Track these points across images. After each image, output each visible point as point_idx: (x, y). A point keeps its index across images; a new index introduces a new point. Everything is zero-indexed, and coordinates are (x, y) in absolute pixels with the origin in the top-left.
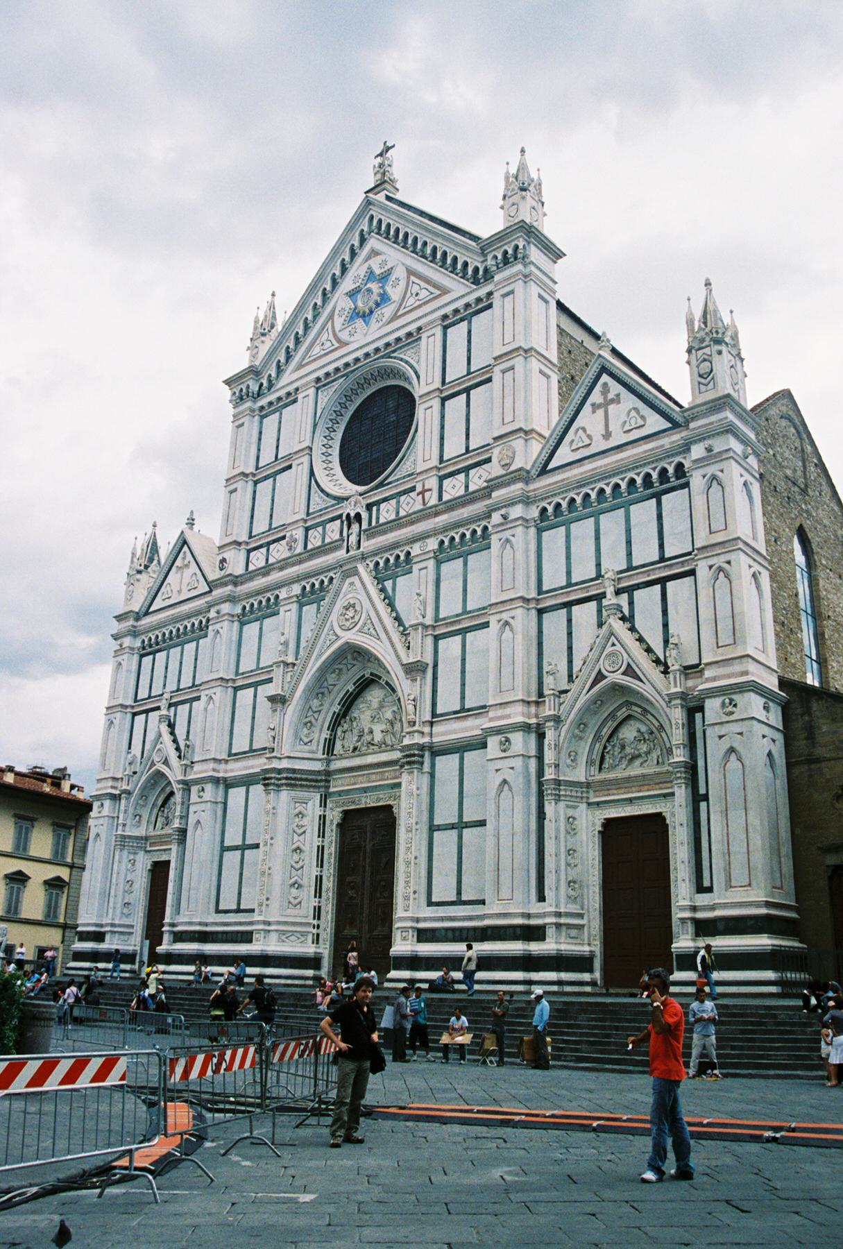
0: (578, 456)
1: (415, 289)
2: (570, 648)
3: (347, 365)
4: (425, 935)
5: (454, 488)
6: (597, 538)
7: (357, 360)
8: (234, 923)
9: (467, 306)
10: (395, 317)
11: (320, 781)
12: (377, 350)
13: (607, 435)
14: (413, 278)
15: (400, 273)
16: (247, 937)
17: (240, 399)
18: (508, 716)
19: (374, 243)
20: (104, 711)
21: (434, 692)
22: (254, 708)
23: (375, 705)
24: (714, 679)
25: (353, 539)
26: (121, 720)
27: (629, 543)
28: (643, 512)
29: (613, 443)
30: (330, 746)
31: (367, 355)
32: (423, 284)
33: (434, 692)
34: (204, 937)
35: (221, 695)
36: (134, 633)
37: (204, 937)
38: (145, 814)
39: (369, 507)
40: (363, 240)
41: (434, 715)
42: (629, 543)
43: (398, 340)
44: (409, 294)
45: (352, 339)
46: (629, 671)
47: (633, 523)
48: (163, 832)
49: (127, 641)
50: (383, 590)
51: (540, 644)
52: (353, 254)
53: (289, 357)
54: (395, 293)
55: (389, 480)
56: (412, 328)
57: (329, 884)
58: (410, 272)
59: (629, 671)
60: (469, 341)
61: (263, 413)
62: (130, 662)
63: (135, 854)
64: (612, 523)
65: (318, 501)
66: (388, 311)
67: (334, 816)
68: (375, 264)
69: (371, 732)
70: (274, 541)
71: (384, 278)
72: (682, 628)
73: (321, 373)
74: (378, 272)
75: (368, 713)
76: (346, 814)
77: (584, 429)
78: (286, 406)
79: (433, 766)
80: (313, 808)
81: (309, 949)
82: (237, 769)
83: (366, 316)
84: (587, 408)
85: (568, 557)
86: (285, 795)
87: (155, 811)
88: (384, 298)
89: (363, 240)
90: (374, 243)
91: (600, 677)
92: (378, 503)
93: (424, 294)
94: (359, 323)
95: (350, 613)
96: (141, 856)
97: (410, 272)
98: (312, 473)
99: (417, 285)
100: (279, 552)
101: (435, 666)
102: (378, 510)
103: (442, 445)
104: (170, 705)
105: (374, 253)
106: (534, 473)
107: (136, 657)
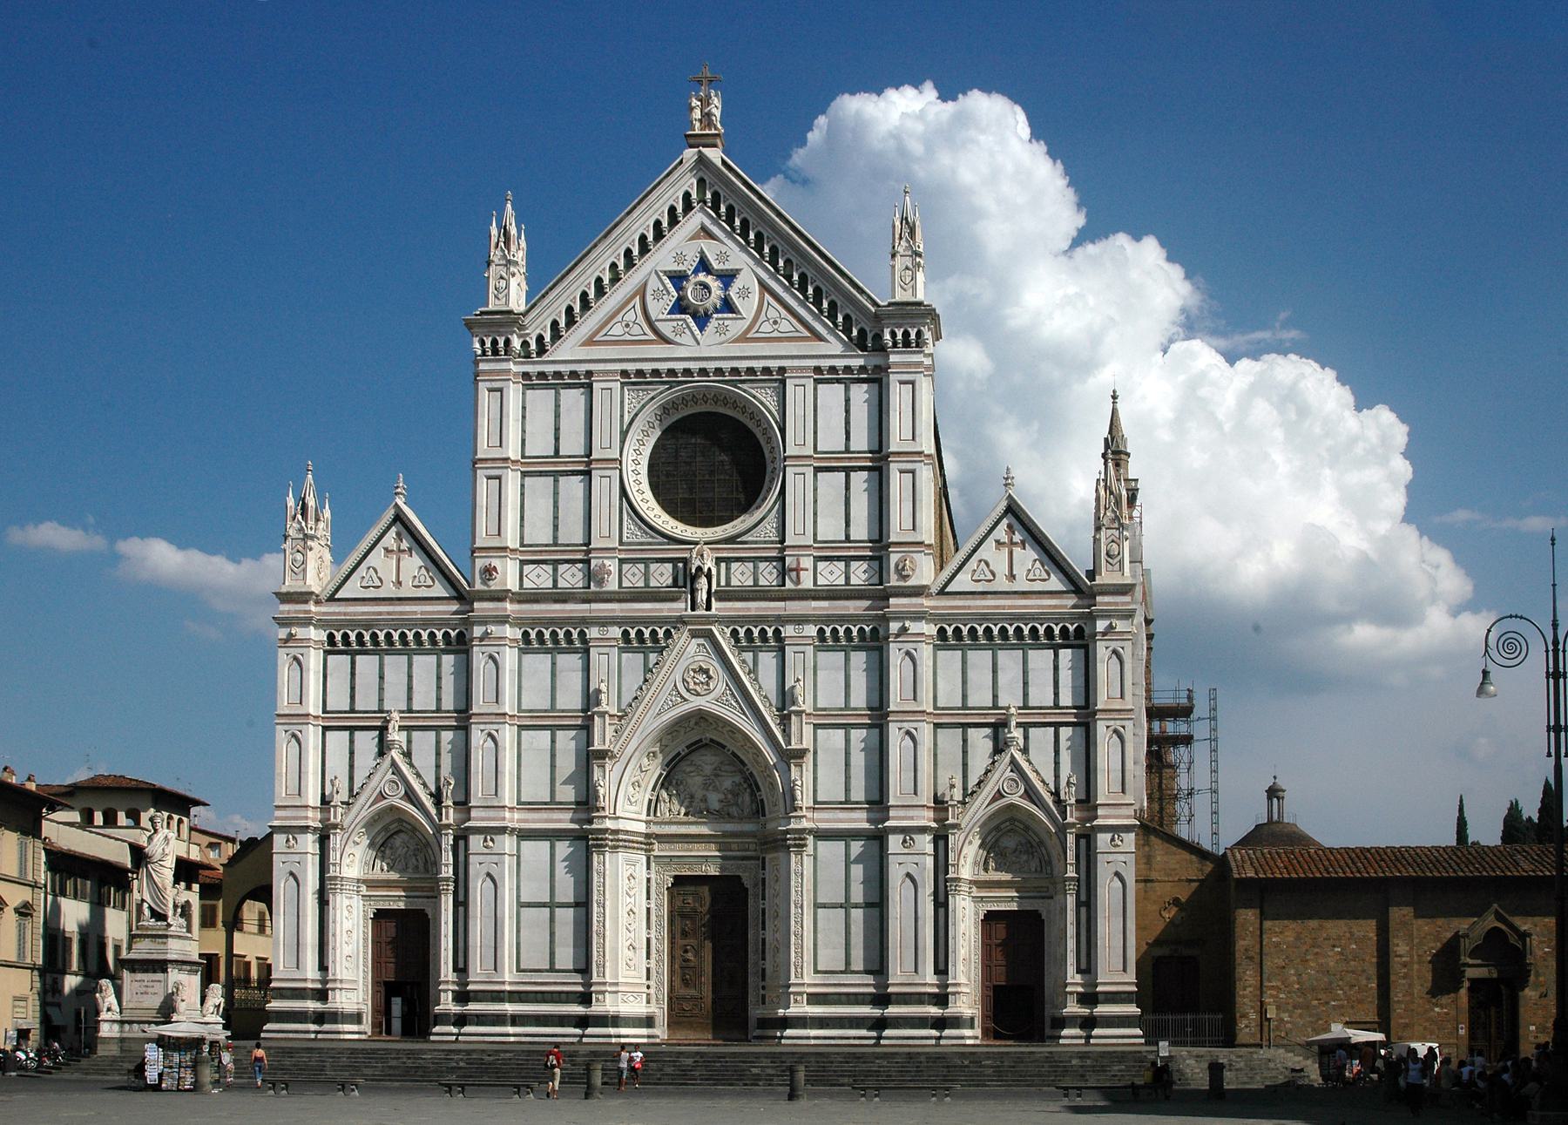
0: (980, 587)
1: (772, 314)
2: (965, 765)
3: (672, 372)
4: (815, 999)
5: (831, 575)
6: (995, 671)
7: (687, 372)
9: (848, 369)
10: (743, 338)
12: (719, 371)
13: (1012, 577)
14: (767, 296)
18: (912, 818)
21: (815, 779)
22: (553, 756)
23: (708, 769)
24: (1105, 817)
25: (702, 596)
27: (1025, 684)
28: (1041, 660)
29: (1016, 587)
31: (703, 372)
32: (784, 312)
33: (815, 779)
39: (718, 560)
40: (688, 207)
41: (815, 802)
42: (1025, 684)
43: (751, 371)
44: (763, 317)
45: (678, 339)
47: (1031, 665)
50: (744, 661)
51: (935, 755)
52: (674, 220)
53: (571, 321)
55: (744, 538)
60: (847, 411)
64: (1009, 661)
65: (631, 531)
66: (736, 327)
68: (711, 250)
69: (704, 800)
70: (567, 561)
71: (727, 278)
74: (716, 265)
75: (698, 780)
76: (679, 881)
77: (987, 564)
78: (569, 386)
79: (815, 849)
80: (641, 872)
82: (538, 821)
83: (702, 320)
84: (990, 542)
85: (964, 682)
86: (622, 855)
88: (728, 306)
89: (688, 207)
91: (999, 795)
92: (728, 560)
93: (785, 326)
95: (702, 678)
98: (623, 493)
99: (774, 310)
100: (571, 577)
101: (815, 753)
102: (728, 569)
103: (815, 522)
104: (401, 728)
106: (934, 590)
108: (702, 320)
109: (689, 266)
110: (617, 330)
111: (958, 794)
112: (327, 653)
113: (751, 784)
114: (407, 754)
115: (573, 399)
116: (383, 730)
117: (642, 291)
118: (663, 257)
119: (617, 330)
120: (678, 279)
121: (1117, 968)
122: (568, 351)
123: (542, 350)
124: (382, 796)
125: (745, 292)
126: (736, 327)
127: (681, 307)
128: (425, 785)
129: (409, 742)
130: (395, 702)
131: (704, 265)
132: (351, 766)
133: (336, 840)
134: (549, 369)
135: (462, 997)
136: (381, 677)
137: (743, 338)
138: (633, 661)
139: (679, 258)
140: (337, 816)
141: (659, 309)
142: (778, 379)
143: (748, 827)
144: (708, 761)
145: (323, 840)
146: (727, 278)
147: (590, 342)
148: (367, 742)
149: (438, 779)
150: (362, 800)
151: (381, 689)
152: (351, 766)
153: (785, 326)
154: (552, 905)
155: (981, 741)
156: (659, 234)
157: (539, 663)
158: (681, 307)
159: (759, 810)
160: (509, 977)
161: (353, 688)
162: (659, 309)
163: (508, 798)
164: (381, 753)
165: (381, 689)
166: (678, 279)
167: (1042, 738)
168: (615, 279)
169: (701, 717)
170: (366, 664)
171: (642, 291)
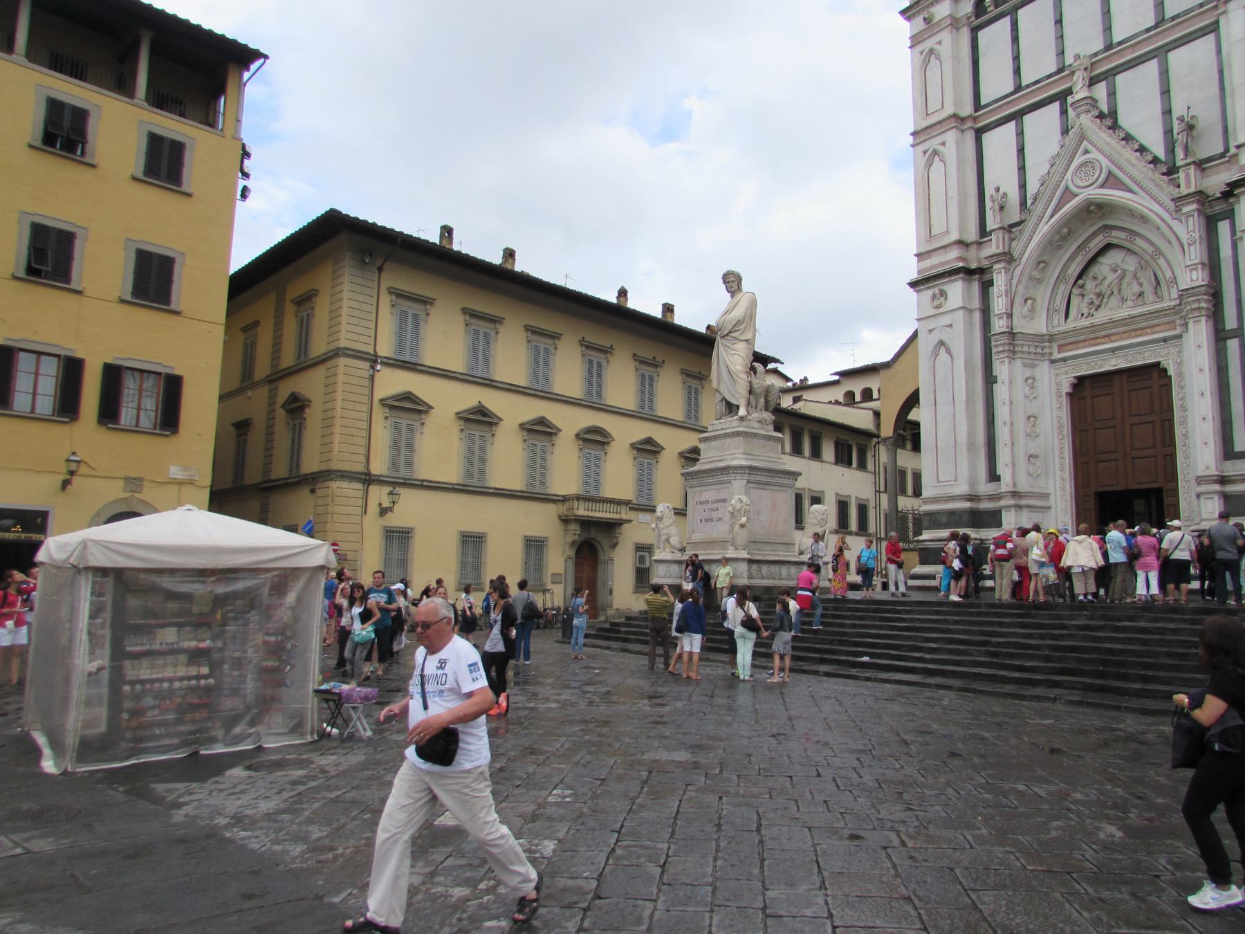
20: (910, 140)
26: (953, 144)
38: (1042, 295)
48: (1085, 323)
62: (951, 45)
63: (1033, 366)
87: (1063, 289)
96: (1044, 371)
104: (1092, 82)
107: (965, 34)
112: (975, 31)
114: (1110, 119)
116: (1062, 97)
124: (1068, 194)
128: (1142, 149)
129: (1112, 94)
132: (1022, 169)
133: (1000, 281)
136: (1059, 22)
149: (1168, 132)
150: (1038, 210)
151: (1060, 37)
152: (1022, 169)
161: (1016, 58)
164: (1065, 131)
165: (1060, 37)
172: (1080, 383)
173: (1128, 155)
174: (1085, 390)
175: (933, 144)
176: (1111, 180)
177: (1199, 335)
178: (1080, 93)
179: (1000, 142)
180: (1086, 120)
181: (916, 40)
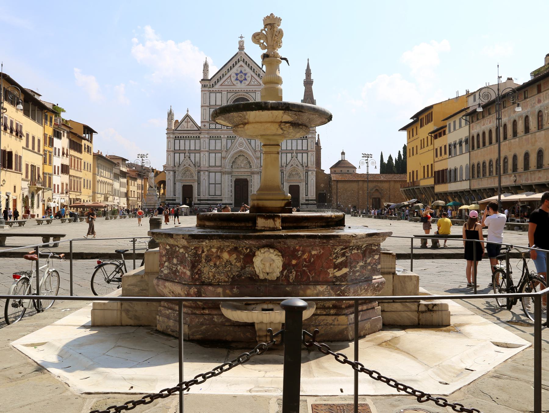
8: (219, 198)
10: (248, 85)
11: (230, 173)
15: (249, 75)
16: (221, 200)
17: (204, 86)
19: (241, 63)
26: (172, 154)
28: (300, 142)
30: (232, 167)
34: (208, 200)
35: (207, 154)
36: (173, 133)
37: (208, 200)
46: (297, 165)
49: (172, 136)
53: (218, 82)
54: (249, 79)
56: (254, 90)
57: (233, 191)
58: (252, 76)
59: (297, 165)
61: (210, 92)
62: (172, 141)
67: (234, 179)
71: (245, 74)
72: (305, 160)
73: (229, 90)
74: (244, 72)
81: (231, 202)
83: (241, 82)
86: (227, 175)
88: (245, 79)
89: (239, 61)
90: (241, 63)
91: (292, 165)
93: (256, 83)
94: (238, 82)
97: (252, 76)
105: (241, 66)
108: (241, 82)
109: (238, 72)
110: (226, 83)
111: (285, 165)
113: (249, 163)
114: (189, 158)
115: (219, 95)
117: (230, 76)
118: (234, 70)
119: (226, 83)
120: (237, 74)
121: (312, 195)
122: (217, 87)
123: (213, 87)
125: (249, 77)
126: (247, 83)
127: (237, 79)
130: (187, 148)
131: (241, 72)
134: (214, 90)
135: (198, 200)
137: (248, 85)
138: (229, 141)
139: (237, 70)
140: (176, 168)
141: (233, 79)
142: (255, 92)
143: (249, 170)
144: (241, 158)
145: (175, 172)
146: (245, 74)
147: (221, 85)
148: (182, 155)
153: (256, 83)
154: (215, 184)
155: (289, 155)
156: (233, 66)
157: (213, 142)
158: (237, 79)
159: (251, 167)
160: (207, 197)
162: (233, 79)
163: (207, 165)
166: (237, 74)
167: (300, 155)
168: (226, 74)
169: (241, 151)
170: (182, 142)
171: (230, 76)
172: (184, 185)
173: (191, 163)
174: (185, 187)
175: (169, 153)
176: (189, 165)
177: (196, 184)
178: (187, 154)
179: (177, 155)
180: (187, 158)
181: (167, 138)
